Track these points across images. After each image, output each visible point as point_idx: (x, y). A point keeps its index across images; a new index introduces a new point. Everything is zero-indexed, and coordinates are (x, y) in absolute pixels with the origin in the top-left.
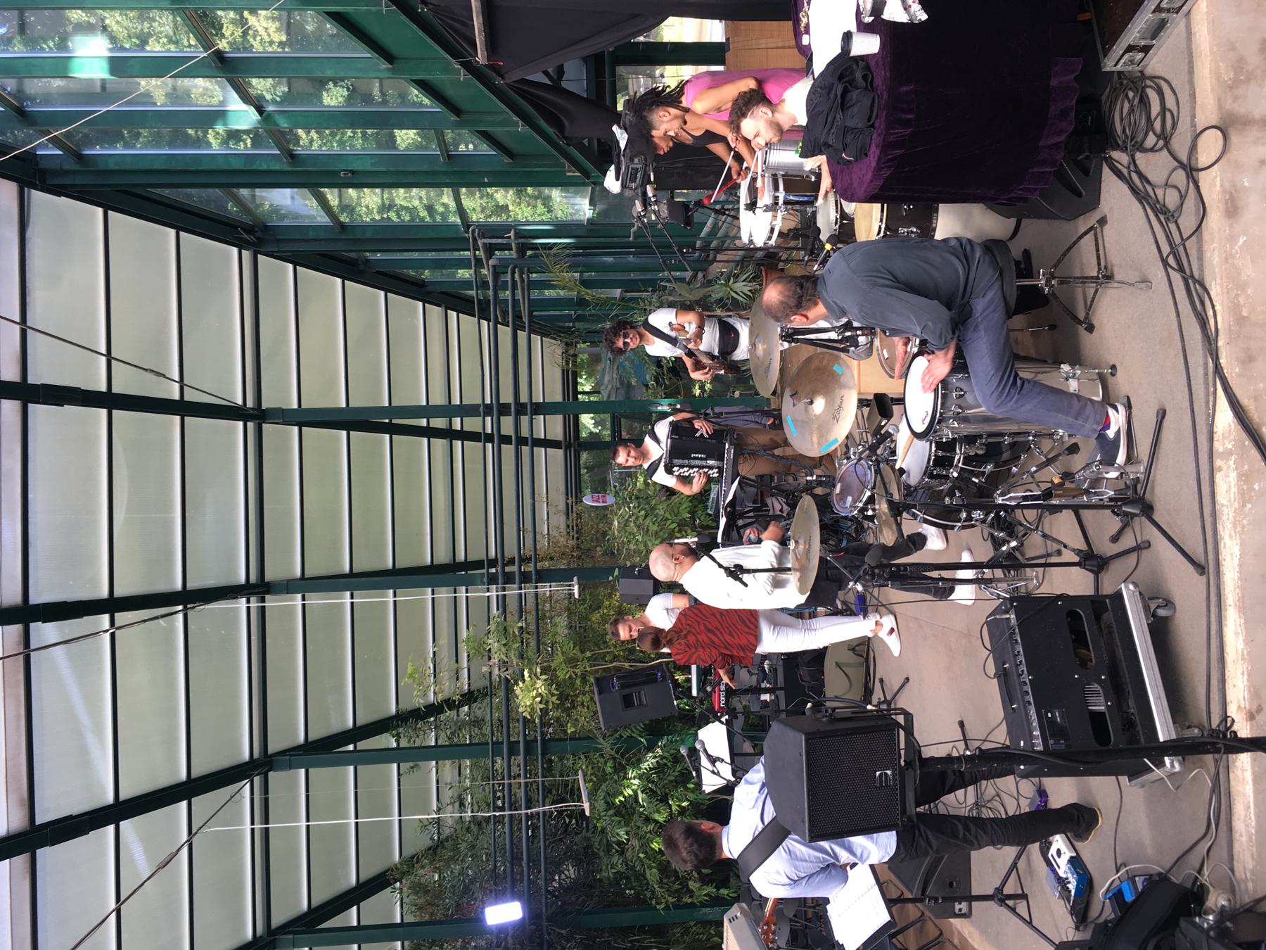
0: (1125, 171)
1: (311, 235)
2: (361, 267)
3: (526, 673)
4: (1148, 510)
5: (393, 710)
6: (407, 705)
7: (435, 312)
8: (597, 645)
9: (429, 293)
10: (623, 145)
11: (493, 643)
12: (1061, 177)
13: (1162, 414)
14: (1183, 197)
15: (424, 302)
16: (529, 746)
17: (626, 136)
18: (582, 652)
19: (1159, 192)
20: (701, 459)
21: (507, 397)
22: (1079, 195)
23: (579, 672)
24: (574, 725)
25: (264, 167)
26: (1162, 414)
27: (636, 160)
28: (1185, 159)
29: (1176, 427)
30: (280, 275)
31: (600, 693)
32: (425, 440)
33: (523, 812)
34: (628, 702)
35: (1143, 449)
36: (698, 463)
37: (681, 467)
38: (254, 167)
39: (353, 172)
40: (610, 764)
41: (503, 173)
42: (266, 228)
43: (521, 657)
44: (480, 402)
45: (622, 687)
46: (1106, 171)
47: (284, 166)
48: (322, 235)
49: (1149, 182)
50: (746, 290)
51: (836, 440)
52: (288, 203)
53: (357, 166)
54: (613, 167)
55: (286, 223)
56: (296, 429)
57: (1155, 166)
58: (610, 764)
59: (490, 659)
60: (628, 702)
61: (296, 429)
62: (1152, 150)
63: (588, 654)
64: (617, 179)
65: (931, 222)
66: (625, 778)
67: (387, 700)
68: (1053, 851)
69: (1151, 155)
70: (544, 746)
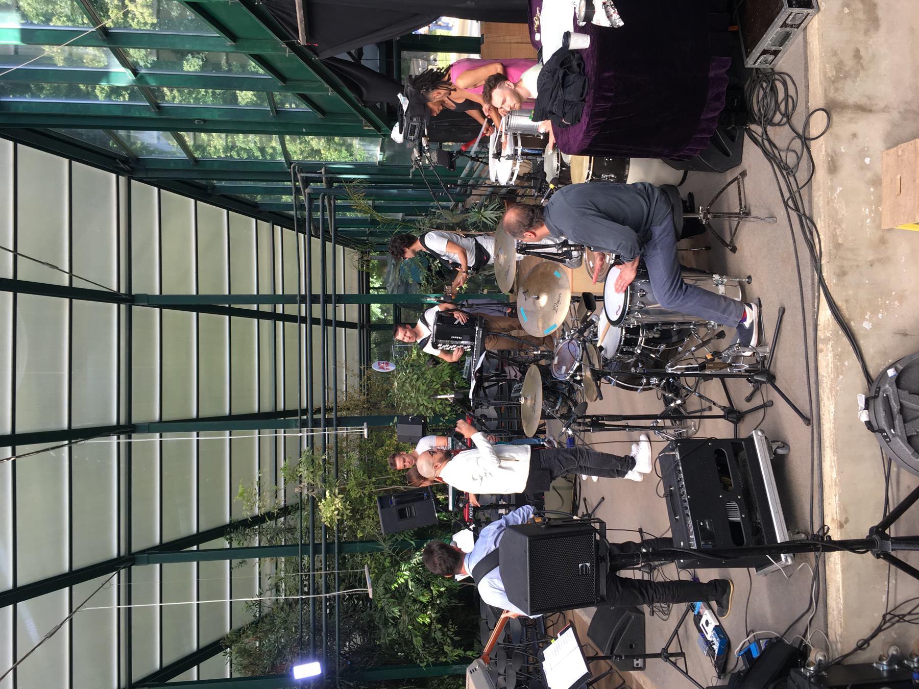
0: (759, 139)
1: (172, 166)
2: (210, 191)
3: (327, 493)
4: (772, 379)
5: (227, 520)
6: (238, 517)
7: (265, 226)
8: (380, 472)
9: (260, 212)
10: (405, 109)
11: (303, 471)
12: (715, 141)
13: (782, 311)
14: (799, 159)
15: (257, 219)
16: (329, 547)
17: (408, 102)
18: (369, 478)
19: (783, 154)
20: (458, 340)
21: (317, 290)
22: (728, 155)
23: (366, 492)
24: (362, 532)
25: (137, 114)
26: (782, 311)
27: (415, 120)
28: (801, 132)
29: (792, 319)
30: (147, 195)
31: (382, 507)
32: (194, 314)
33: (324, 595)
34: (402, 514)
35: (769, 336)
36: (457, 343)
37: (444, 344)
38: (129, 115)
39: (205, 121)
40: (388, 560)
41: (317, 126)
42: (138, 160)
43: (324, 481)
44: (297, 293)
45: (398, 503)
46: (747, 139)
47: (152, 114)
48: (180, 167)
49: (776, 147)
50: (493, 216)
51: (555, 325)
52: (155, 142)
53: (207, 116)
54: (397, 124)
55: (154, 157)
56: (158, 310)
57: (780, 136)
58: (388, 560)
59: (301, 482)
60: (402, 514)
61: (158, 310)
62: (779, 124)
63: (374, 479)
64: (401, 133)
65: (624, 170)
66: (399, 570)
67: (222, 513)
68: (703, 622)
69: (777, 128)
70: (340, 547)
